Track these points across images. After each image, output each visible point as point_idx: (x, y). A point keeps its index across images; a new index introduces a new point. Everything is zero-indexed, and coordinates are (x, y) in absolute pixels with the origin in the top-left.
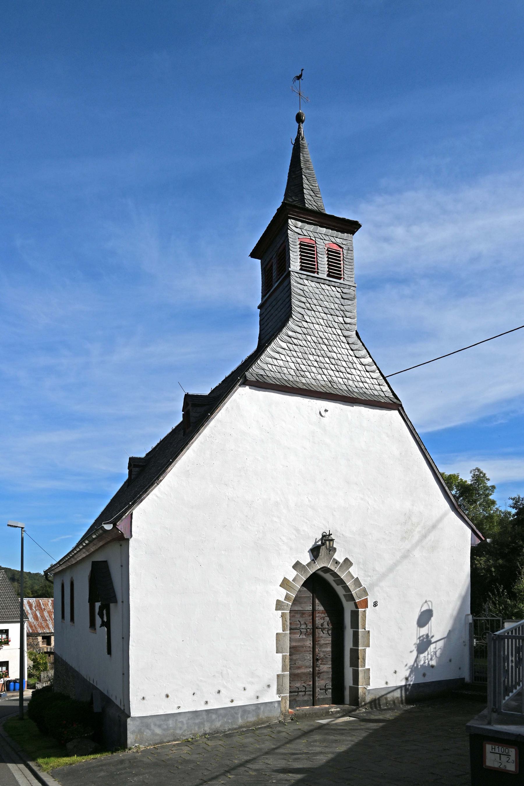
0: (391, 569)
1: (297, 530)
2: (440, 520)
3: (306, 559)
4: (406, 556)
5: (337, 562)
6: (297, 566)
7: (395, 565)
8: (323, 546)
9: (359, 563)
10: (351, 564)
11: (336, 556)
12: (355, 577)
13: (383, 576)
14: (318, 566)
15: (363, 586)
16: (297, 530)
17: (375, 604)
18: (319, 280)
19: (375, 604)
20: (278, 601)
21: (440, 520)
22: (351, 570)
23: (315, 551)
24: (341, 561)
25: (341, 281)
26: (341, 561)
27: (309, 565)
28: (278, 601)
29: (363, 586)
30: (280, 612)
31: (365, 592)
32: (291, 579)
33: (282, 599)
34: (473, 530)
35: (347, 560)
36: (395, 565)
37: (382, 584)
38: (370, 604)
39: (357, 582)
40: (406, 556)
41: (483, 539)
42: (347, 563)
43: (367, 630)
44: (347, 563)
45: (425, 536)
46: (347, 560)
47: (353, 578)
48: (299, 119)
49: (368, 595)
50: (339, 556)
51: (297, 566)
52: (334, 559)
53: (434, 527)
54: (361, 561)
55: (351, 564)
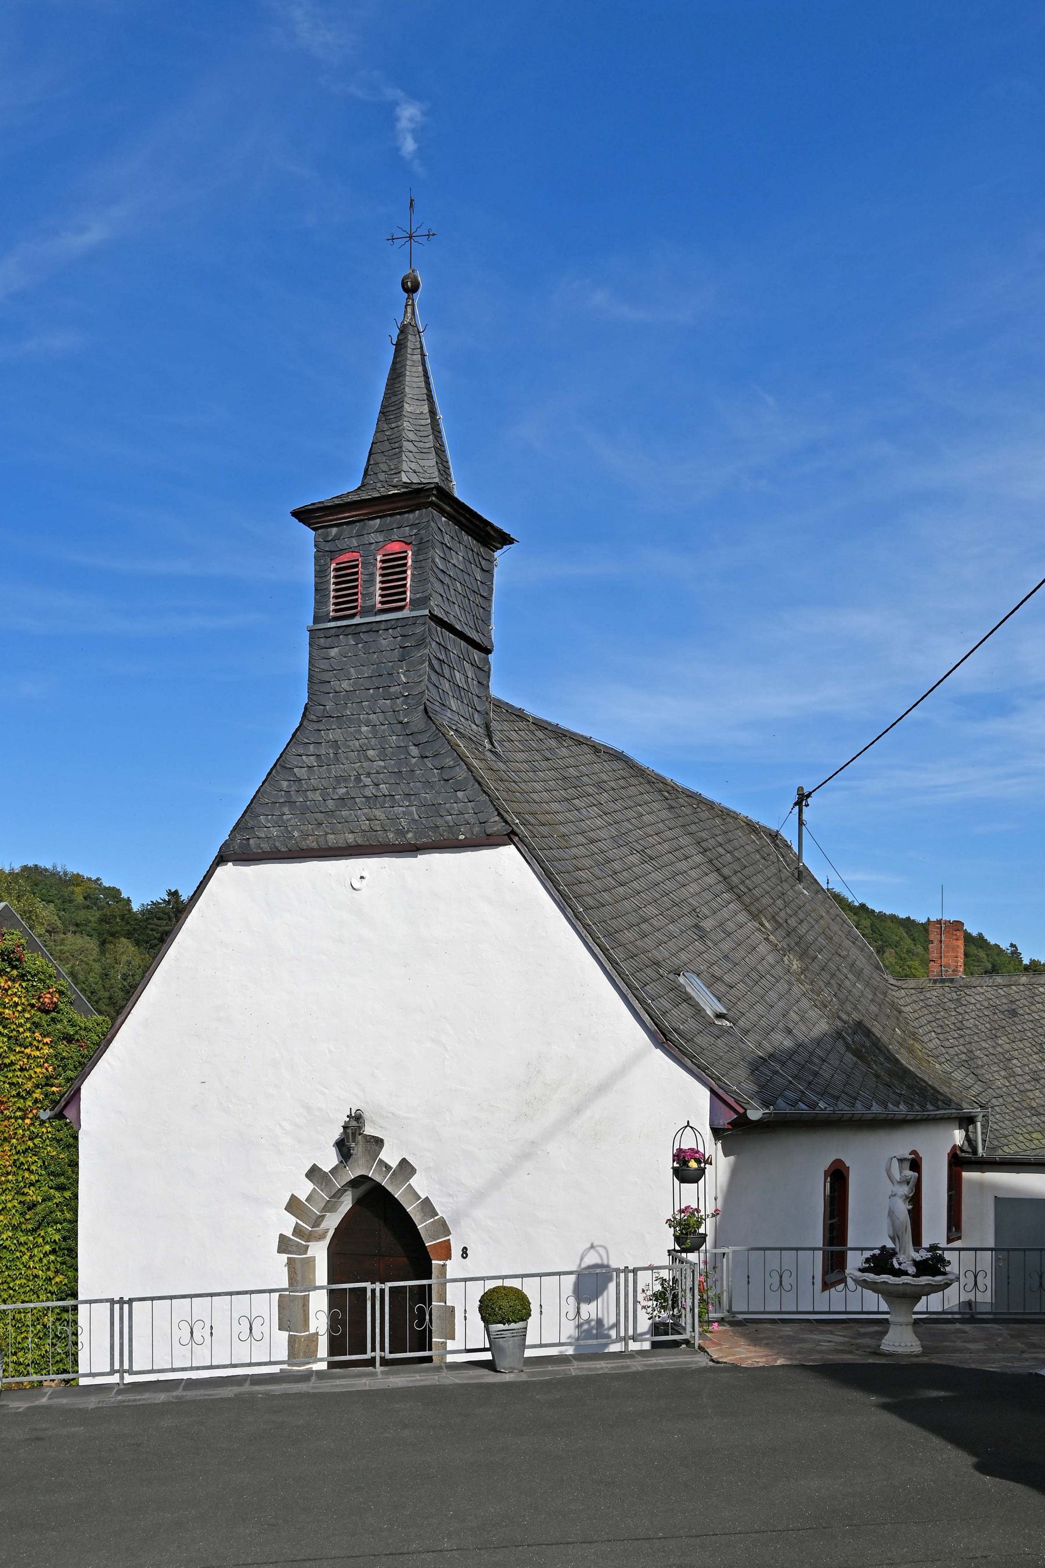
1: (308, 1109)
2: (622, 1071)
3: (329, 1160)
4: (527, 1153)
5: (388, 1167)
6: (314, 1173)
7: (506, 1172)
8: (353, 1139)
9: (427, 1169)
10: (413, 1171)
11: (383, 1156)
12: (423, 1197)
13: (479, 1197)
14: (351, 1174)
15: (440, 1215)
16: (308, 1109)
17: (465, 1253)
18: (359, 629)
19: (465, 1253)
20: (282, 1238)
21: (622, 1071)
22: (414, 1181)
24: (394, 1164)
25: (406, 613)
26: (394, 1164)
27: (334, 1171)
28: (282, 1238)
29: (440, 1215)
30: (284, 1257)
31: (443, 1227)
32: (303, 1198)
33: (289, 1233)
34: (712, 1091)
35: (404, 1162)
36: (506, 1172)
39: (427, 1207)
40: (527, 1153)
41: (741, 1111)
42: (406, 1168)
43: (448, 1304)
44: (406, 1168)
45: (578, 1111)
46: (404, 1162)
47: (420, 1198)
48: (411, 288)
49: (449, 1233)
50: (390, 1156)
51: (314, 1173)
52: (381, 1161)
53: (602, 1088)
54: (432, 1165)
55: (413, 1171)
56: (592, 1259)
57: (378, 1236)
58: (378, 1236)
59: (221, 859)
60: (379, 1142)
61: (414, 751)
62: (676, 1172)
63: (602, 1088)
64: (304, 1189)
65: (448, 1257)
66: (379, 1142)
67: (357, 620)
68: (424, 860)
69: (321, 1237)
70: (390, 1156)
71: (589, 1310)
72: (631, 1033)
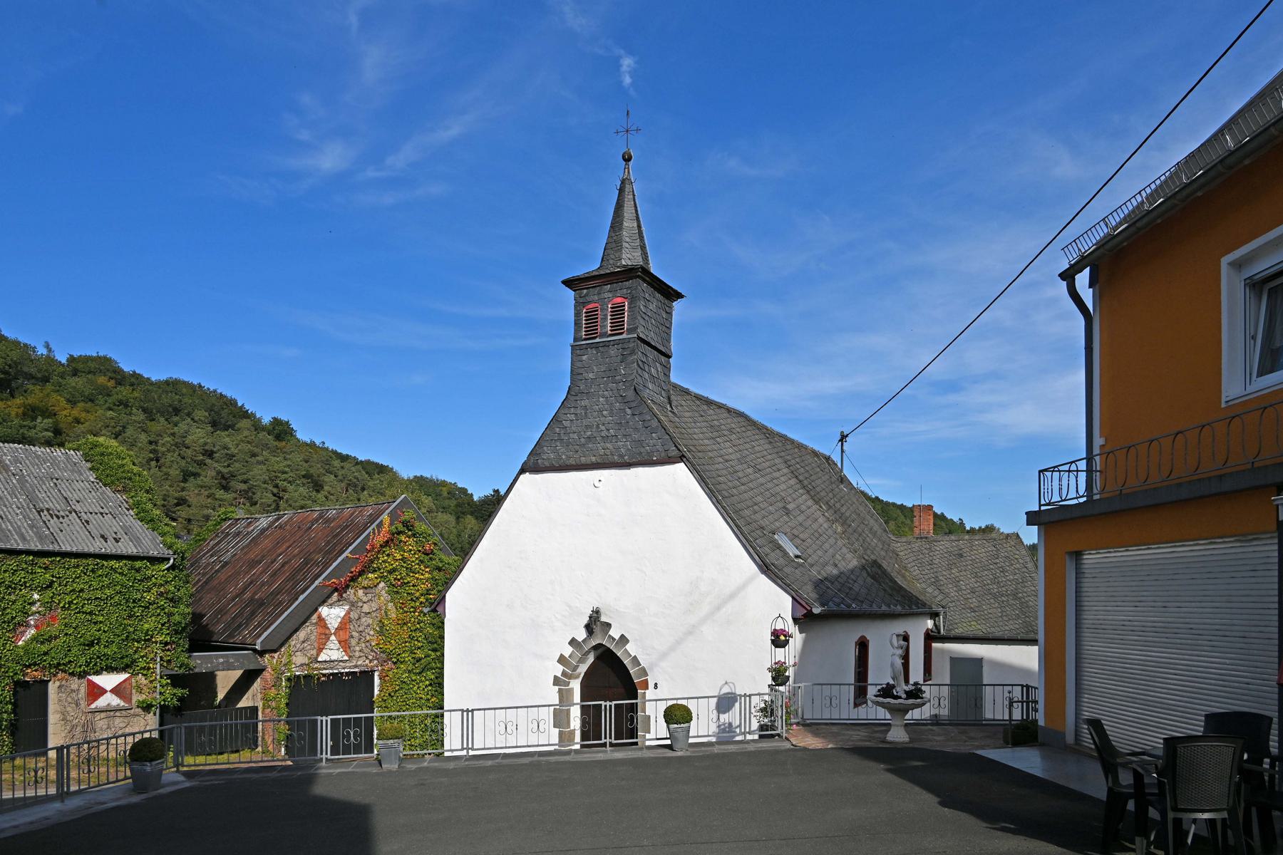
0: (672, 649)
1: (570, 607)
3: (581, 635)
6: (573, 642)
7: (679, 642)
8: (595, 623)
9: (636, 640)
10: (628, 641)
11: (611, 633)
13: (664, 656)
16: (570, 607)
22: (628, 647)
23: (589, 628)
24: (617, 637)
25: (624, 336)
30: (557, 688)
31: (644, 672)
33: (559, 675)
36: (679, 642)
37: (663, 664)
38: (651, 685)
39: (635, 660)
42: (623, 640)
44: (623, 640)
45: (718, 608)
48: (627, 158)
50: (615, 633)
51: (573, 642)
53: (732, 596)
55: (628, 641)
56: (726, 690)
57: (608, 676)
58: (608, 676)
59: (522, 471)
60: (609, 625)
61: (629, 411)
62: (773, 642)
63: (732, 596)
64: (568, 651)
65: (647, 688)
66: (609, 625)
67: (597, 340)
68: (634, 471)
69: (577, 677)
70: (615, 633)
71: (725, 718)
72: (750, 567)
